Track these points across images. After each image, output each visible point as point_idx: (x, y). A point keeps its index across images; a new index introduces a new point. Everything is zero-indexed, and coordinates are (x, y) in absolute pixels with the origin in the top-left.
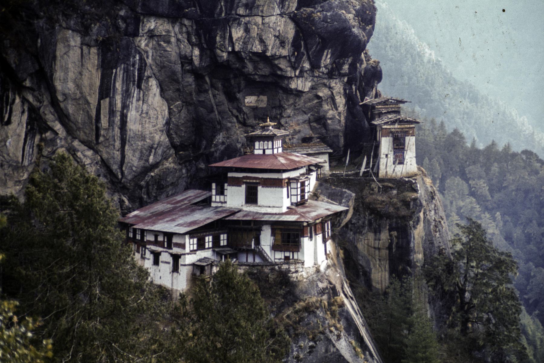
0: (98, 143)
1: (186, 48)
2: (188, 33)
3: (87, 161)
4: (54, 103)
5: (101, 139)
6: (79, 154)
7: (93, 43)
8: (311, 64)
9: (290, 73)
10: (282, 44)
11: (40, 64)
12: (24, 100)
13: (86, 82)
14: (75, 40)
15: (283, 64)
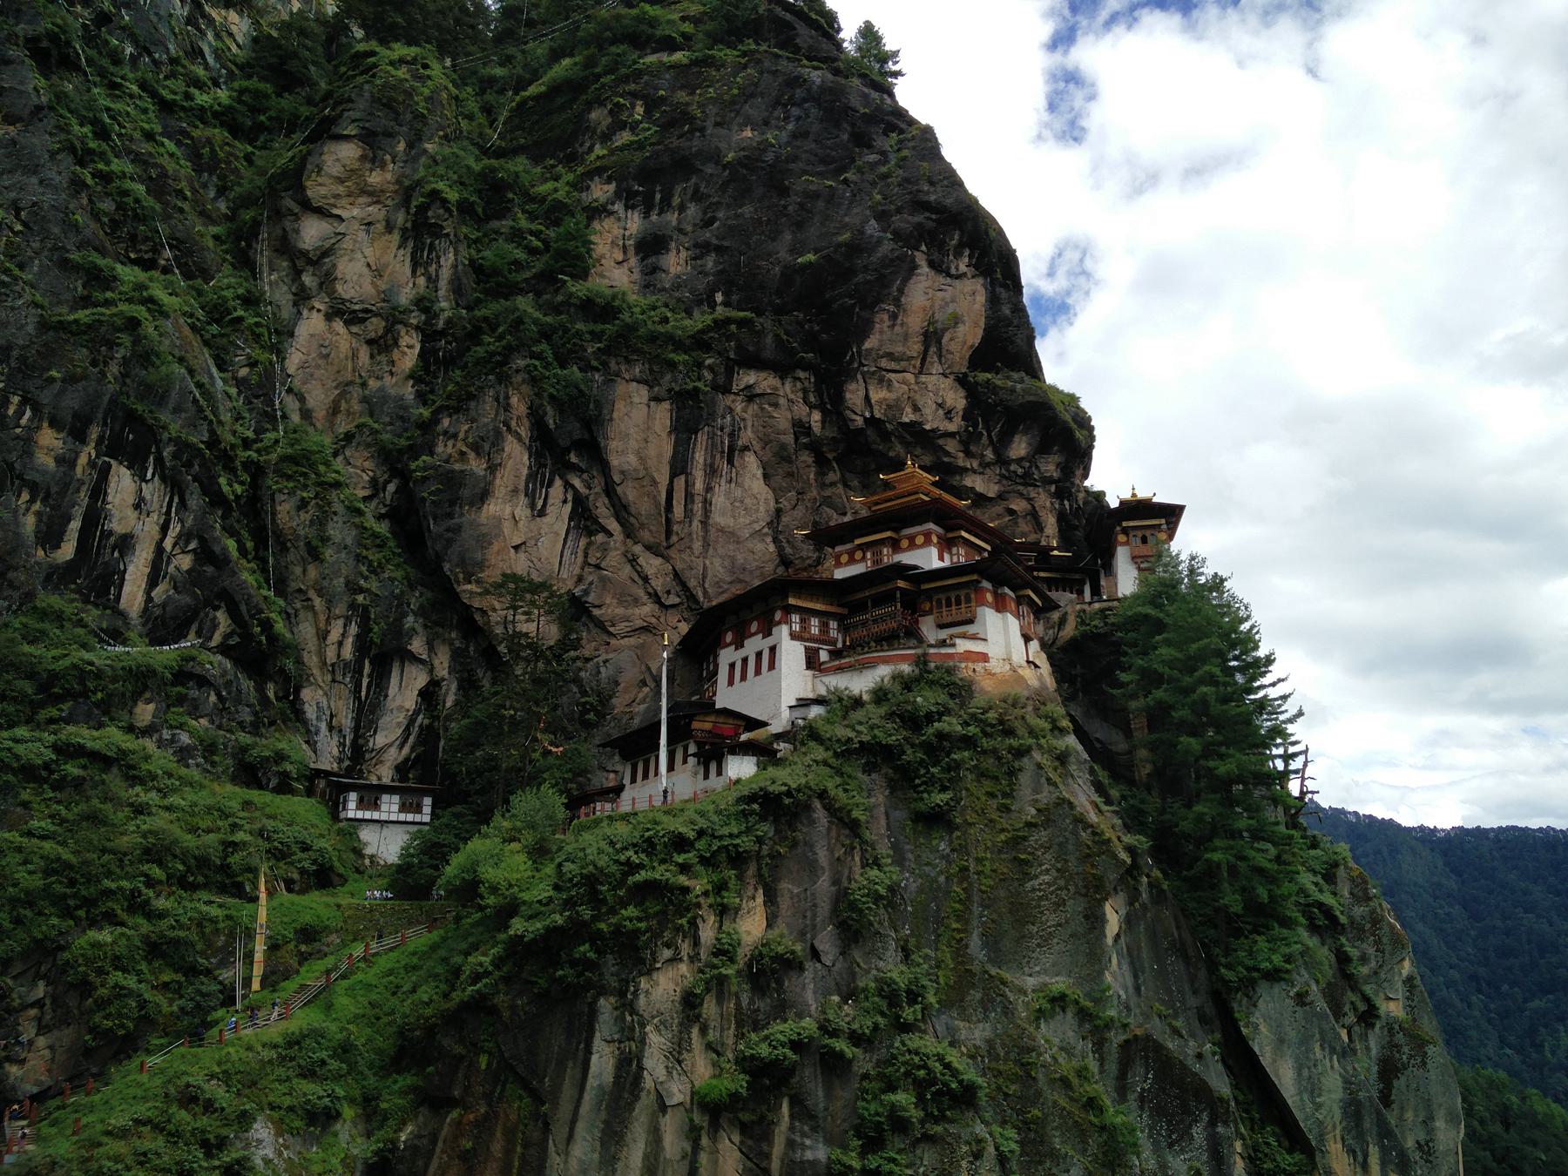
0: (668, 547)
1: (801, 410)
2: (805, 391)
3: (650, 571)
4: (610, 491)
5: (674, 538)
6: (641, 561)
7: (664, 394)
8: (995, 452)
9: (962, 461)
10: (949, 415)
11: (590, 431)
12: (568, 485)
13: (652, 451)
14: (640, 394)
15: (951, 446)
